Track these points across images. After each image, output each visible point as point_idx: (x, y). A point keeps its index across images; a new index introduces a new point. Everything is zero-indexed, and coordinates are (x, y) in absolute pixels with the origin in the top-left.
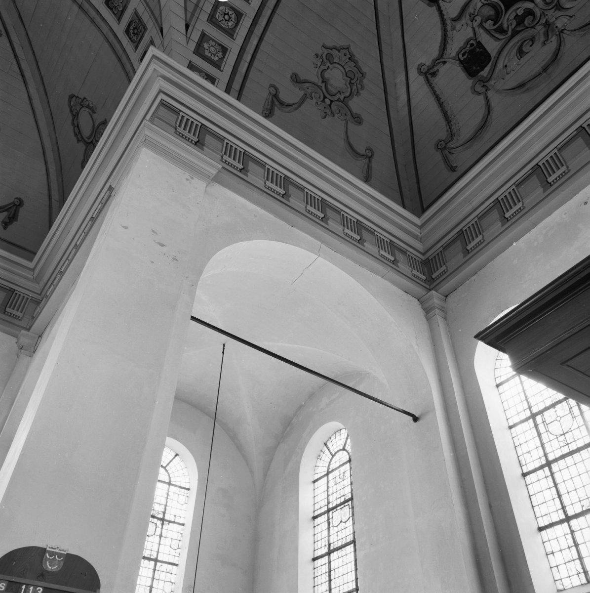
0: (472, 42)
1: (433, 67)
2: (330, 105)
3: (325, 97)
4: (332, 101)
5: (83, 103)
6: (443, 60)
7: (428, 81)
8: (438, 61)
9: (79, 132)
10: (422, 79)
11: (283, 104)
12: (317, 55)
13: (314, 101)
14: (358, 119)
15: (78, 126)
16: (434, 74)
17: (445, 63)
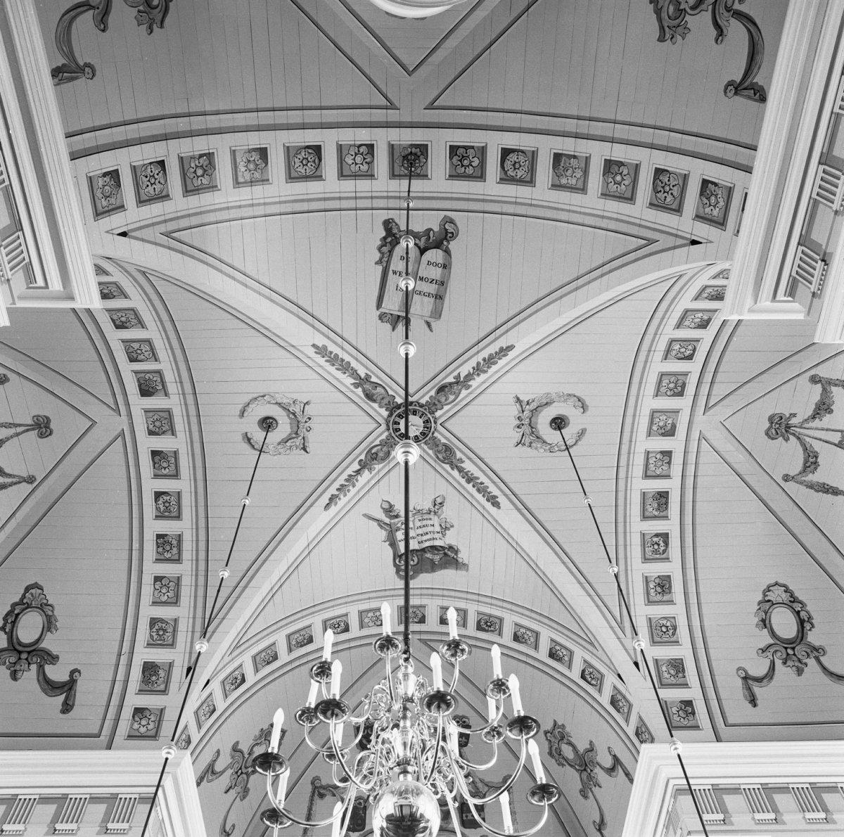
0: (362, 801)
1: (324, 789)
2: (239, 776)
3: (241, 769)
4: (242, 773)
5: (44, 608)
6: (335, 792)
7: (312, 800)
8: (331, 789)
9: (14, 623)
10: (309, 788)
11: (213, 773)
12: (262, 729)
13: (232, 771)
14: (245, 792)
15: (17, 615)
16: (322, 796)
17: (334, 795)
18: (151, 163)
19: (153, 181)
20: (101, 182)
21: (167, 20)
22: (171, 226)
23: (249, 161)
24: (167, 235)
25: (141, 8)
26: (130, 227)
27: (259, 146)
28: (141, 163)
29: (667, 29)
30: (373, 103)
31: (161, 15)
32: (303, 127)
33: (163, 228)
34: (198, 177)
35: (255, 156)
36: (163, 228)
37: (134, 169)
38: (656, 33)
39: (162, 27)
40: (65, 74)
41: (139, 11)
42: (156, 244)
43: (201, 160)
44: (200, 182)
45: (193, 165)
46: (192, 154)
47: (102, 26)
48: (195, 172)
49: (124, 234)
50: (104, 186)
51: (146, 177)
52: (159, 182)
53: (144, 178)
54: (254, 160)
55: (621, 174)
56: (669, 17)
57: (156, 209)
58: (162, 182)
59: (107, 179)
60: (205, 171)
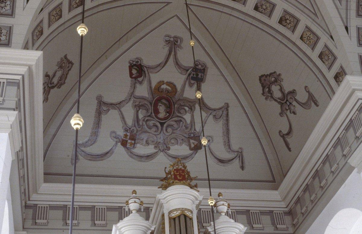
18: (306, 43)
19: (309, 38)
20: (327, 63)
21: (273, 72)
22: (313, 16)
23: (264, 10)
24: (316, 15)
25: (279, 82)
26: (328, 36)
27: (257, 12)
28: (308, 47)
29: (64, 59)
30: (196, 7)
31: (273, 74)
32: (233, 9)
33: (316, 19)
34: (290, 20)
35: (260, 9)
36: (316, 19)
37: (313, 49)
38: (69, 57)
39: (275, 72)
40: (314, 100)
41: (281, 82)
42: (323, 18)
43: (285, 24)
44: (290, 18)
45: (289, 26)
46: (287, 30)
47: (295, 91)
48: (290, 23)
49: (332, 37)
50: (327, 60)
51: (310, 42)
52: (306, 35)
53: (311, 42)
54: (262, 8)
55: (76, 3)
56: (64, 63)
57: (315, 28)
58: (305, 33)
59: (324, 60)
60: (286, 20)
